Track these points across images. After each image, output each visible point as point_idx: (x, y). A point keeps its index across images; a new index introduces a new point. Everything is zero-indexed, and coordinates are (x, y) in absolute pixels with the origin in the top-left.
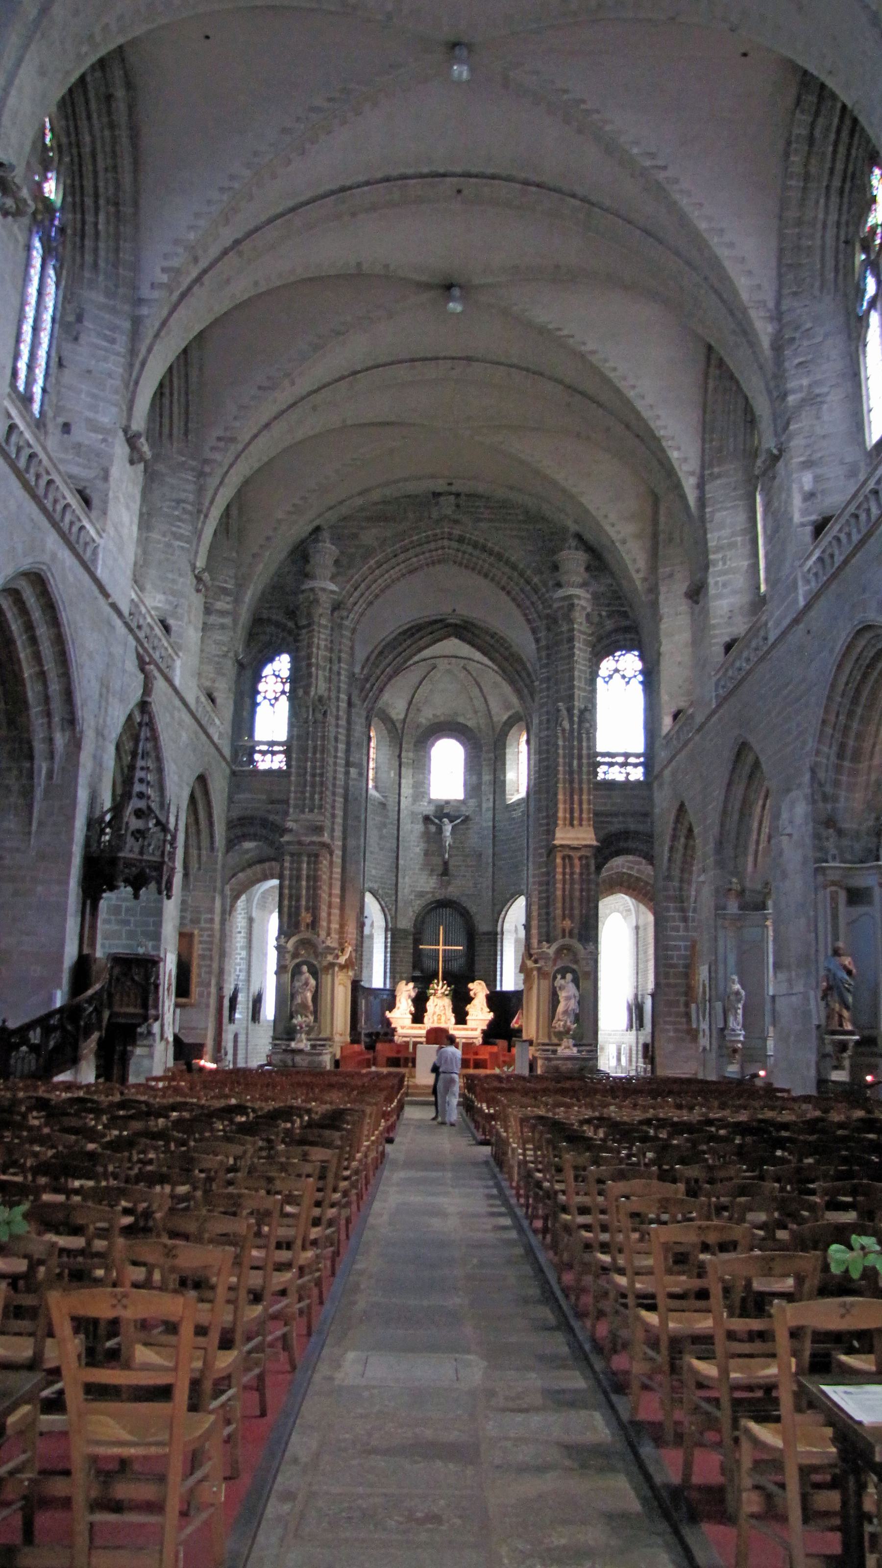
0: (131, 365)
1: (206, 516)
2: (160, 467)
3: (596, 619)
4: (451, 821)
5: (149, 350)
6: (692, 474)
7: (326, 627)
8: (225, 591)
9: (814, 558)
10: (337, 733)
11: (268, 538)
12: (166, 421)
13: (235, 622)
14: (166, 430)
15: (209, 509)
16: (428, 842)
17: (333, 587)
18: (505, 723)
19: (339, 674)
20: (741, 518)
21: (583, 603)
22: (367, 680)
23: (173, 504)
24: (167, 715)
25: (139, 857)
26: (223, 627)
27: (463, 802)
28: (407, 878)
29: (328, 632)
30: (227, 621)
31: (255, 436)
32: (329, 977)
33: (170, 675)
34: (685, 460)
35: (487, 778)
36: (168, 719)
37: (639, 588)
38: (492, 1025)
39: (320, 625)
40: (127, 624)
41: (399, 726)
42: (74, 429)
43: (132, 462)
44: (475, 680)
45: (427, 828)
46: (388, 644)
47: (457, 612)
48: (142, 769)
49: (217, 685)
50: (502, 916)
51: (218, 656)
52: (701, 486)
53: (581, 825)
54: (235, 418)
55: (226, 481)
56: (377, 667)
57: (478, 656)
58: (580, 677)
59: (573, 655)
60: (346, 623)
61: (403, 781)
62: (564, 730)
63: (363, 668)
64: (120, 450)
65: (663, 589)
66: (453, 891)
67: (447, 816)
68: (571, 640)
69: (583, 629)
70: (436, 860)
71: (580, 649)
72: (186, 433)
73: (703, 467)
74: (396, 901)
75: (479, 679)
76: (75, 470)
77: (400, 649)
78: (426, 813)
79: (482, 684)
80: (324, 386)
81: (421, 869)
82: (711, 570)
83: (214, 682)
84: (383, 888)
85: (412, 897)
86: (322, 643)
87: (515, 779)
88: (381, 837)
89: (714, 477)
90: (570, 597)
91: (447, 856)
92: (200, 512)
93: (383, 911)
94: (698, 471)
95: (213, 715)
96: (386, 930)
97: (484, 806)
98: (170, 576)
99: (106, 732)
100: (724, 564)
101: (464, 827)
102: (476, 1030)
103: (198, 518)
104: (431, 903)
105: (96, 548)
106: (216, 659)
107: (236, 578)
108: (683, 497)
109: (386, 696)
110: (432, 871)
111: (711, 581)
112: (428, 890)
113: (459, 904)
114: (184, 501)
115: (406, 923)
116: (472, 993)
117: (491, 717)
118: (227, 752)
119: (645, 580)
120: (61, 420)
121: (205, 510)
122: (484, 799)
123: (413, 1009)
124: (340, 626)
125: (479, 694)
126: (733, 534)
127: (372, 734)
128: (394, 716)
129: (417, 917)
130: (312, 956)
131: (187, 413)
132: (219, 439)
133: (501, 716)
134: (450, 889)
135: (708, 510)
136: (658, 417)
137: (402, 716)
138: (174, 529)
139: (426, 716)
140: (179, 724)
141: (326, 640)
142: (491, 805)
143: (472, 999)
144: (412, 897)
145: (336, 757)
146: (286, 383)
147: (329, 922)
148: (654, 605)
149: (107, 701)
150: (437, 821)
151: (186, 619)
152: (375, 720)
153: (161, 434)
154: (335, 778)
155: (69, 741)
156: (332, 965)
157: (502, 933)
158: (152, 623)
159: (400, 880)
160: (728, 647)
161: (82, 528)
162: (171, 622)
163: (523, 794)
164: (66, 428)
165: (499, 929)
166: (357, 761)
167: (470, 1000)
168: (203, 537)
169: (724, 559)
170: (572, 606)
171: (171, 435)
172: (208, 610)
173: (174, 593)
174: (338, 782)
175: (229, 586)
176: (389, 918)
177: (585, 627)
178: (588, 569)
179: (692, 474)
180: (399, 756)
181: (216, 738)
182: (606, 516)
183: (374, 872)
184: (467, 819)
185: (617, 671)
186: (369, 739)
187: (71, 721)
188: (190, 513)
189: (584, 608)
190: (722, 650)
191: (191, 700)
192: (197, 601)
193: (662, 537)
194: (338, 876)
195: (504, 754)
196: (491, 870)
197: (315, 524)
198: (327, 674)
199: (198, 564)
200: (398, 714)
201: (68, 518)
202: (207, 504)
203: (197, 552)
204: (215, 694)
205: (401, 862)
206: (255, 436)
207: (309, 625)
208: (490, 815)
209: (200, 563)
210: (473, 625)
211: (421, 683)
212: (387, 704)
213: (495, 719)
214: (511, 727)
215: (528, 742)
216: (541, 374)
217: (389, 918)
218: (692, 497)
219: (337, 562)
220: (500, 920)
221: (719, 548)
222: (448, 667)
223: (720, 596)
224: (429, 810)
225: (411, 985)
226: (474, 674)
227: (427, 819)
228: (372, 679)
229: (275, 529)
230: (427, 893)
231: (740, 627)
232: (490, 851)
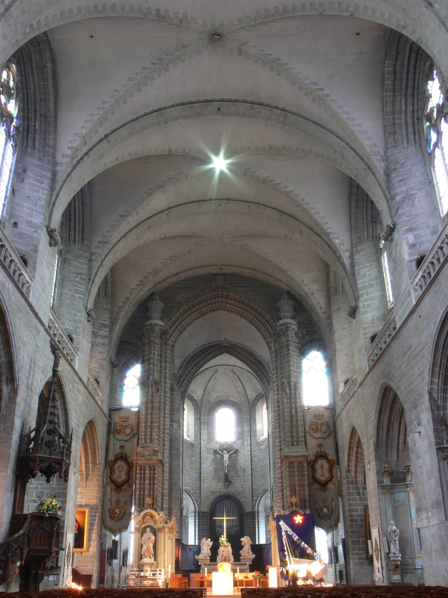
0: (51, 195)
1: (93, 282)
2: (69, 256)
3: (300, 335)
4: (228, 453)
5: (61, 188)
6: (347, 251)
7: (158, 344)
8: (104, 325)
9: (419, 277)
10: (165, 400)
11: (127, 298)
12: (72, 233)
13: (110, 341)
14: (72, 238)
15: (94, 278)
16: (216, 464)
17: (161, 323)
18: (255, 399)
19: (165, 369)
20: (374, 271)
21: (293, 327)
22: (181, 376)
23: (75, 275)
24: (70, 384)
25: (49, 456)
26: (103, 344)
27: (234, 442)
28: (206, 484)
29: (159, 346)
30: (106, 341)
31: (119, 241)
32: (163, 534)
33: (73, 364)
34: (343, 244)
35: (246, 428)
36: (71, 387)
37: (322, 317)
38: (254, 561)
39: (154, 343)
40: (46, 330)
41: (199, 403)
42: (19, 226)
43: (51, 245)
44: (238, 377)
45: (216, 457)
46: (192, 357)
47: (227, 340)
48: (52, 407)
49: (100, 375)
50: (257, 503)
51: (100, 359)
52: (352, 257)
53: (298, 445)
54: (108, 231)
55: (104, 263)
56: (187, 369)
57: (240, 363)
58: (293, 365)
59: (290, 353)
60: (169, 342)
61: (202, 432)
62: (286, 394)
63: (179, 370)
64: (44, 238)
65: (335, 316)
66: (231, 490)
67: (226, 449)
68: (288, 345)
69: (293, 340)
70: (222, 474)
71: (293, 350)
72: (83, 240)
73: (352, 247)
74: (200, 496)
75: (240, 377)
76: (20, 246)
77: (198, 360)
78: (215, 448)
79: (242, 379)
80: (154, 215)
81: (212, 479)
82: (360, 299)
83: (98, 373)
84: (193, 490)
85: (209, 494)
86: (156, 352)
87: (261, 428)
88: (191, 462)
89: (358, 252)
90: (286, 324)
91: (226, 471)
92: (90, 280)
94: (349, 249)
95: (98, 390)
97: (246, 443)
98: (73, 312)
99: (33, 388)
100: (367, 295)
101: (235, 455)
102: (246, 564)
103: (89, 283)
104: (219, 497)
105: (29, 287)
106: (100, 361)
107: (111, 319)
108: (342, 264)
109: (192, 387)
110: (219, 479)
111: (361, 305)
112: (217, 490)
113: (234, 497)
114: (81, 274)
115: (205, 508)
116: (243, 543)
117: (247, 397)
118: (106, 411)
119: (325, 312)
120: (12, 221)
121: (92, 278)
122: (245, 439)
123: (210, 554)
124: (166, 344)
125: (241, 385)
126: (371, 280)
127: (185, 407)
128: (196, 397)
129: (212, 505)
130: (153, 523)
131: (83, 230)
132: (100, 242)
133: (252, 395)
134: (229, 489)
135: (356, 268)
136: (327, 223)
137: (200, 398)
138: (76, 288)
139: (213, 397)
140: (78, 391)
141: (158, 351)
142: (249, 443)
143: (243, 547)
144: (209, 494)
145: (165, 413)
146: (134, 213)
147: (162, 503)
148: (330, 326)
149: (34, 370)
150: (220, 452)
151: (81, 334)
152: (187, 400)
153: (69, 240)
154: (164, 425)
155: (11, 391)
156: (164, 527)
157: (258, 512)
158: (62, 334)
159: (202, 485)
160: (373, 339)
161: (21, 275)
162: (74, 336)
163: (266, 436)
164: (15, 224)
165: (256, 510)
166: (177, 419)
167: (242, 547)
168: (91, 292)
169: (367, 293)
170: (287, 327)
171: (75, 241)
172: (94, 335)
173: (75, 321)
174: (166, 427)
175: (106, 323)
177: (295, 339)
178: (294, 309)
179: (347, 251)
180: (200, 419)
181: (99, 403)
182: (303, 281)
183: (188, 481)
184: (237, 451)
185: (312, 367)
186: (184, 409)
187: (12, 379)
188: (85, 280)
189: (294, 329)
190: (369, 340)
191: (85, 380)
192: (88, 326)
193: (332, 290)
194: (167, 478)
195: (255, 415)
196: (250, 478)
197: (151, 291)
198: (159, 369)
199: (88, 307)
200: (198, 396)
201: (13, 267)
202: (93, 275)
203: (88, 301)
204: (99, 380)
205: (202, 475)
206: (119, 241)
207: (149, 343)
208: (249, 448)
209: (90, 306)
210: (235, 346)
211: (209, 380)
212: (193, 392)
213: (249, 397)
214: (258, 401)
215: (267, 408)
216: (265, 206)
217: (196, 505)
218: (347, 263)
219: (163, 311)
220: (257, 505)
221: (364, 288)
222: (224, 371)
223: (365, 313)
224: (216, 447)
225: (209, 540)
226: (238, 374)
227: (215, 452)
228: (184, 376)
229: (131, 293)
230: (217, 491)
231: (378, 327)
232: (250, 468)
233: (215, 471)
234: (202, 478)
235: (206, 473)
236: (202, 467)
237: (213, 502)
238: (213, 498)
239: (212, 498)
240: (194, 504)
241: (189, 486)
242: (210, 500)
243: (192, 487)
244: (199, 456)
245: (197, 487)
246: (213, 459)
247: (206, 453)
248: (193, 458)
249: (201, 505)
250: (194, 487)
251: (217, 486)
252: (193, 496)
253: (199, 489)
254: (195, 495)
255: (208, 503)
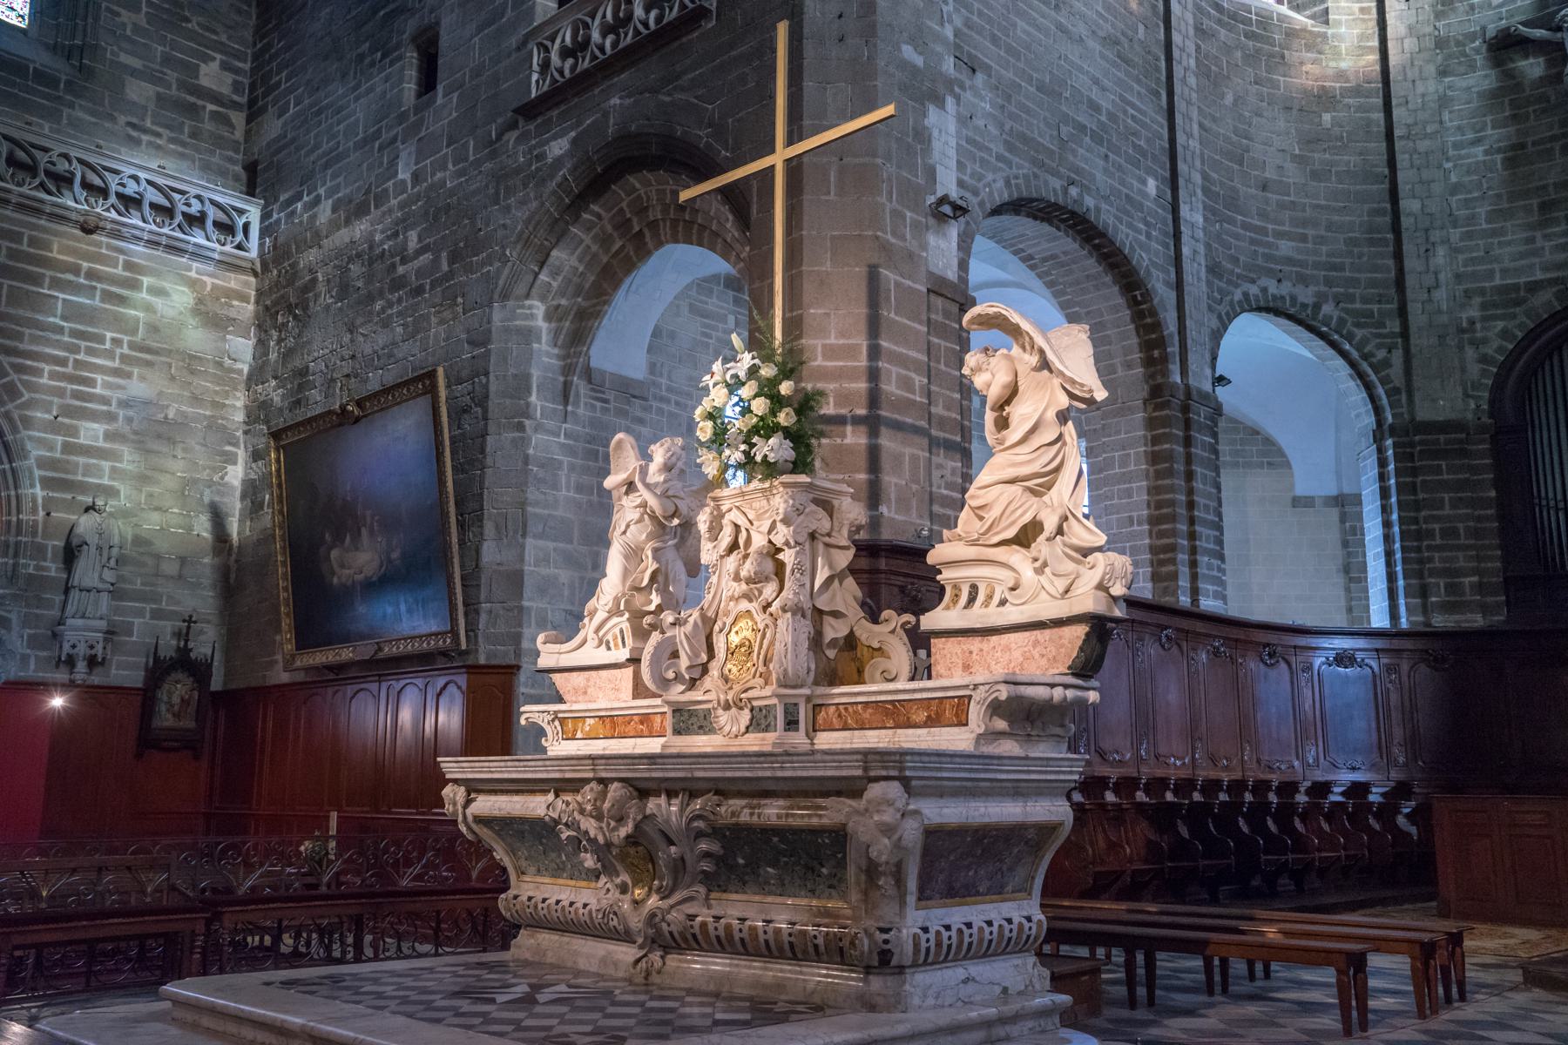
28: (1441, 251)
45: (1508, 75)
74: (1405, 334)
85: (1474, 312)
93: (1361, 376)
96: (1378, 437)
144: (1474, 312)
150: (1539, 33)
159: (1411, 263)
176: (1380, 391)
205: (1409, 205)
217: (1380, 391)
230: (1534, 287)
233: (1511, 163)
234: (1405, 222)
235: (1437, 188)
236: (1402, 159)
237: (1513, 357)
238: (1505, 334)
239: (1497, 337)
240: (1368, 387)
241: (1303, 280)
242: (1489, 350)
243: (1329, 282)
244: (1379, 101)
245: (1372, 283)
246: (1494, 98)
247: (1431, 69)
248: (1327, 117)
249: (1417, 381)
250: (1353, 282)
251: (1535, 253)
252: (1350, 338)
253: (1392, 291)
254: (1359, 333)
255: (1474, 370)
